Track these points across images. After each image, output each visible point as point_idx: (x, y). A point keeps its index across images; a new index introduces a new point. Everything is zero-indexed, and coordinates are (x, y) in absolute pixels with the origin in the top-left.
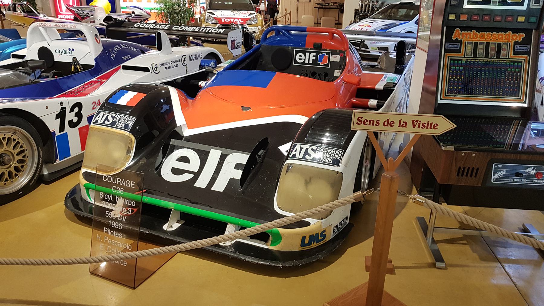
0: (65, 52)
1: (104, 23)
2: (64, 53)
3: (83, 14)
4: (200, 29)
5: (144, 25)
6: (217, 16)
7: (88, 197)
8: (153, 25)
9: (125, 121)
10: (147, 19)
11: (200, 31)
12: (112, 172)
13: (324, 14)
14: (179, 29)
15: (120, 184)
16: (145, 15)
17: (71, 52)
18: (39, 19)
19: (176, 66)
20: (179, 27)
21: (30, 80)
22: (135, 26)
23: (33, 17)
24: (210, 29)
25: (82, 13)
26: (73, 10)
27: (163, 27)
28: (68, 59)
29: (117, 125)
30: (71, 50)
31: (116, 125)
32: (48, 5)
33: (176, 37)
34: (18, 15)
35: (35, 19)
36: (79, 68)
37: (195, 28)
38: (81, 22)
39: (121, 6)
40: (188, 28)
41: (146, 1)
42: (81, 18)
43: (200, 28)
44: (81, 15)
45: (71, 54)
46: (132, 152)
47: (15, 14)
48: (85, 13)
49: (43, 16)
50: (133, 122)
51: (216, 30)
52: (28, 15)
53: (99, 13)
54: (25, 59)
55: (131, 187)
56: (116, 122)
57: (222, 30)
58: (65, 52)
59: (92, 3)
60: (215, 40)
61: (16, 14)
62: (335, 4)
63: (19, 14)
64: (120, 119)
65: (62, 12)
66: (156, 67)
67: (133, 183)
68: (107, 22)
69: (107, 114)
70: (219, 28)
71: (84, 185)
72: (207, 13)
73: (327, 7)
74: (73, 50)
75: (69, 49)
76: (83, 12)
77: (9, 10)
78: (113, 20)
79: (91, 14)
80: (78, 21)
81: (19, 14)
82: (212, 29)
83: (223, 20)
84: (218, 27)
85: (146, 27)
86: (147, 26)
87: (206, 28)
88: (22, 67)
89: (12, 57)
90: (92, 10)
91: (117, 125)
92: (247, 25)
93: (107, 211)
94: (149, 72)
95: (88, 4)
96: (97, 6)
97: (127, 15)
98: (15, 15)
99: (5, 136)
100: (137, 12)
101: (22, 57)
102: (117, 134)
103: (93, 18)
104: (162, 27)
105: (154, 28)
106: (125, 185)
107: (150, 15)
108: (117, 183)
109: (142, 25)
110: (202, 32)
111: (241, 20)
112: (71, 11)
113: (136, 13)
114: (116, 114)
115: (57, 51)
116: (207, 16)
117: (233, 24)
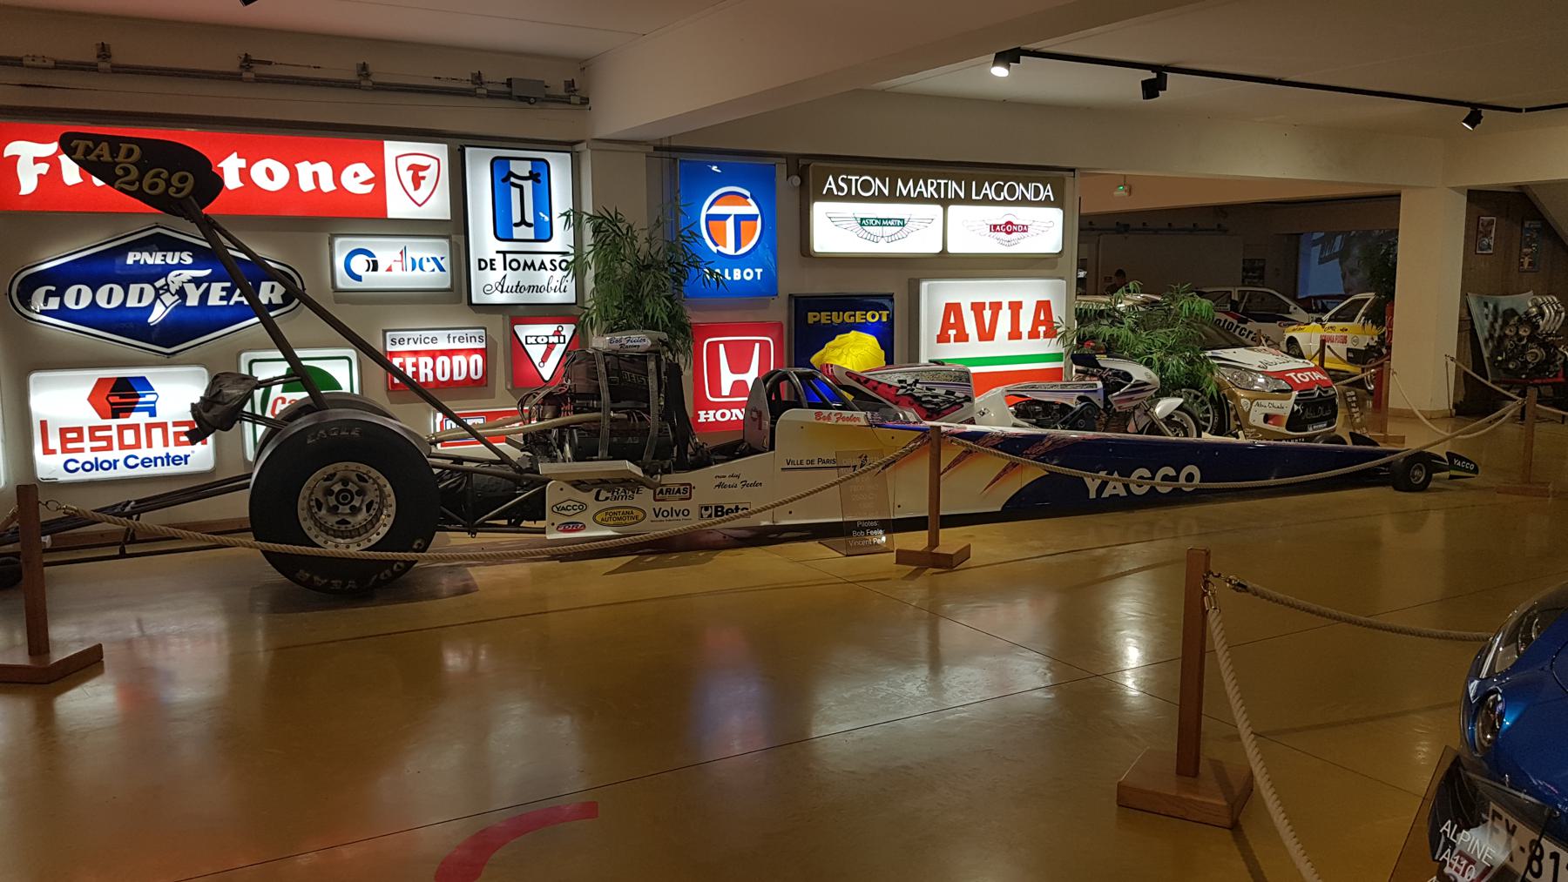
35: (920, 433)
48: (940, 391)
59: (821, 352)
61: (834, 419)
63: (844, 419)
76: (927, 389)
79: (963, 395)
81: (844, 419)
98: (826, 422)
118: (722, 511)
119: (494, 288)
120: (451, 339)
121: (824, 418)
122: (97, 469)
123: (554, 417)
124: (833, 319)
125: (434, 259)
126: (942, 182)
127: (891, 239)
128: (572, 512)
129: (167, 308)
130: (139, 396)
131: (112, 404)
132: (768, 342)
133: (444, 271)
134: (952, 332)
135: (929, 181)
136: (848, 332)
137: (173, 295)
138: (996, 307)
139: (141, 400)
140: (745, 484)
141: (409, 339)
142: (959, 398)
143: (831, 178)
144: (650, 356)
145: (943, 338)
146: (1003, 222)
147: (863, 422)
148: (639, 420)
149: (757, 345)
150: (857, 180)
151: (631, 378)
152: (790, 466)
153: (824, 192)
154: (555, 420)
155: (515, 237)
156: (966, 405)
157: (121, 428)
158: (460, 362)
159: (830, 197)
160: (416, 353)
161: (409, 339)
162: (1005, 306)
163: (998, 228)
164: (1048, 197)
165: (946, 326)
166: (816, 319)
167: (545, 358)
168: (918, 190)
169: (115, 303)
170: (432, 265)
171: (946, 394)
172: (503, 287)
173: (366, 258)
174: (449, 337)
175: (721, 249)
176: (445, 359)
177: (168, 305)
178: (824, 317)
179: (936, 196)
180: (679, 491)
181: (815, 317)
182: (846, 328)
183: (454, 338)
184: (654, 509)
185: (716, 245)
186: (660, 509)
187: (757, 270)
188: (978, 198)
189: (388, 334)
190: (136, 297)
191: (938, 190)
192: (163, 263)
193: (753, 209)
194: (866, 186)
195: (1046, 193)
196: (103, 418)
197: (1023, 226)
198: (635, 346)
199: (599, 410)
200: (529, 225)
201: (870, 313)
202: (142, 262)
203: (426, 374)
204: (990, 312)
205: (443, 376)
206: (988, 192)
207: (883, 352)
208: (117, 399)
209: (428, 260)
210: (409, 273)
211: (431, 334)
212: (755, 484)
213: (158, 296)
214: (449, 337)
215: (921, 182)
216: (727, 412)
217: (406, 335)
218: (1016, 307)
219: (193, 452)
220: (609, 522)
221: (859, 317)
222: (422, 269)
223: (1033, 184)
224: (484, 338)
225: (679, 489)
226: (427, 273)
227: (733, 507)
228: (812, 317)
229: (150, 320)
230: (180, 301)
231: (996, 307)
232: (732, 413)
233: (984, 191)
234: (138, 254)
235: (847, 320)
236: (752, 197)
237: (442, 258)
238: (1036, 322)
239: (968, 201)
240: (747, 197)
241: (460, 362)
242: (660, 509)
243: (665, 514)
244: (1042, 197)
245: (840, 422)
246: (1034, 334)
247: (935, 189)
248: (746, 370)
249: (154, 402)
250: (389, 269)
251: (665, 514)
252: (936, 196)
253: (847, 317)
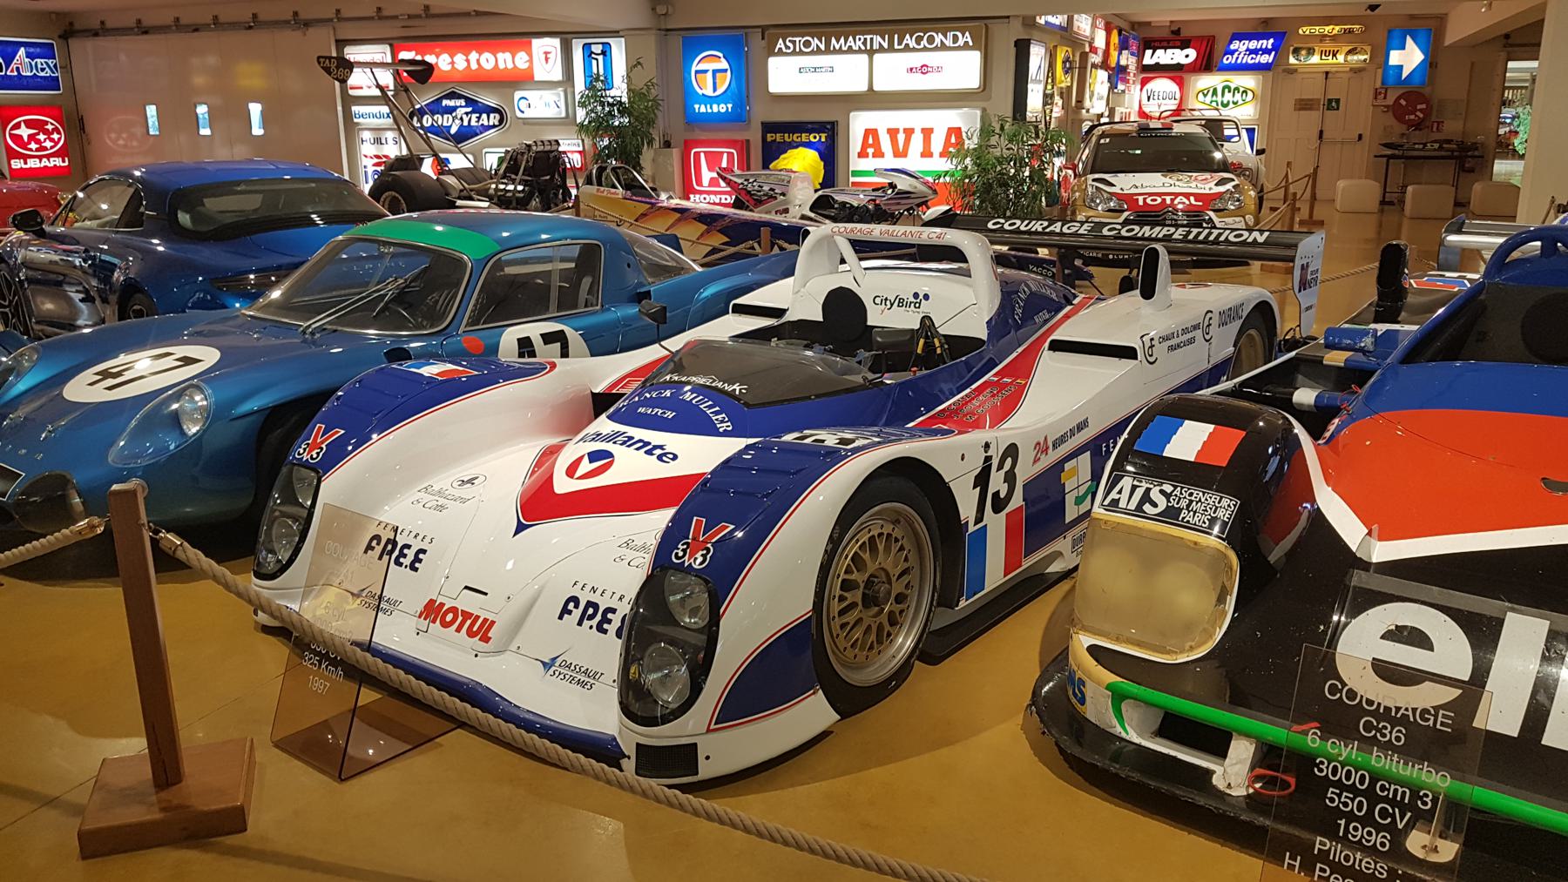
0: (901, 303)
1: (812, 215)
2: (898, 306)
3: (760, 191)
4: (1190, 232)
5: (1015, 224)
6: (1122, 189)
7: (1115, 721)
8: (1041, 224)
9: (1208, 509)
10: (927, 201)
11: (1191, 237)
12: (1182, 652)
13: (1404, 175)
14: (1006, 227)
15: (1393, 714)
16: (922, 192)
17: (920, 303)
18: (660, 205)
19: (1191, 341)
20: (1006, 221)
21: (865, 379)
22: (990, 225)
23: (643, 199)
24: (1222, 231)
25: (756, 188)
26: (736, 182)
27: (1074, 229)
28: (908, 320)
29: (1184, 518)
30: (921, 297)
31: (1180, 519)
32: (670, 169)
33: (1009, 250)
34: (609, 195)
35: (649, 206)
36: (937, 344)
37: (1173, 229)
38: (751, 210)
39: (851, 169)
40: (1151, 229)
41: (919, 155)
42: (753, 202)
43: (1187, 229)
44: (754, 194)
45: (919, 307)
46: (1231, 599)
47: (603, 192)
48: (766, 188)
49: (667, 198)
50: (1233, 512)
51: (1241, 235)
52: (633, 194)
53: (801, 190)
54: (788, 317)
55: (1438, 726)
56: (1180, 510)
57: (1261, 235)
58: (901, 303)
59: (776, 161)
60: (1111, 257)
61: (605, 193)
62: (1445, 146)
64: (1191, 501)
65: (702, 186)
66: (1152, 346)
67: (1444, 716)
68: (819, 212)
69: (1145, 485)
70: (1126, 222)
71: (1109, 685)
72: (1090, 182)
73: (1422, 153)
74: (926, 297)
75: (916, 295)
76: (759, 186)
77: (589, 181)
78: (836, 206)
80: (746, 210)
82: (1228, 232)
83: (1141, 199)
84: (1126, 219)
85: (1022, 228)
86: (1026, 226)
87: (1207, 231)
88: (776, 339)
89: (733, 312)
90: (783, 181)
91: (1184, 518)
92: (1211, 214)
93: (1331, 789)
94: (1136, 358)
95: (766, 166)
96: (794, 170)
97: (874, 194)
99: (883, 531)
100: (903, 184)
101: (778, 313)
102: (1189, 543)
103: (785, 202)
104: (1068, 228)
105: (1048, 230)
106: (1412, 719)
107: (935, 192)
108: (1381, 711)
109: (1010, 225)
110: (1195, 241)
111: (1196, 200)
112: (729, 183)
113: (899, 187)
114: (1175, 487)
115: (878, 300)
116: (1090, 189)
117: (1169, 212)
126: (868, 37)
134: (870, 151)
135: (857, 37)
138: (909, 132)
143: (781, 41)
145: (863, 154)
146: (919, 66)
147: (620, 196)
150: (800, 41)
153: (776, 51)
159: (780, 53)
163: (914, 70)
164: (966, 42)
165: (865, 145)
168: (848, 44)
179: (863, 48)
188: (900, 47)
190: (444, 120)
191: (865, 43)
193: (724, 64)
194: (807, 44)
195: (965, 39)
201: (812, 136)
206: (909, 42)
215: (851, 38)
218: (927, 133)
223: (952, 33)
228: (769, 137)
231: (909, 132)
233: (905, 42)
235: (795, 139)
236: (724, 57)
239: (891, 49)
240: (720, 58)
244: (961, 42)
247: (863, 43)
252: (863, 48)
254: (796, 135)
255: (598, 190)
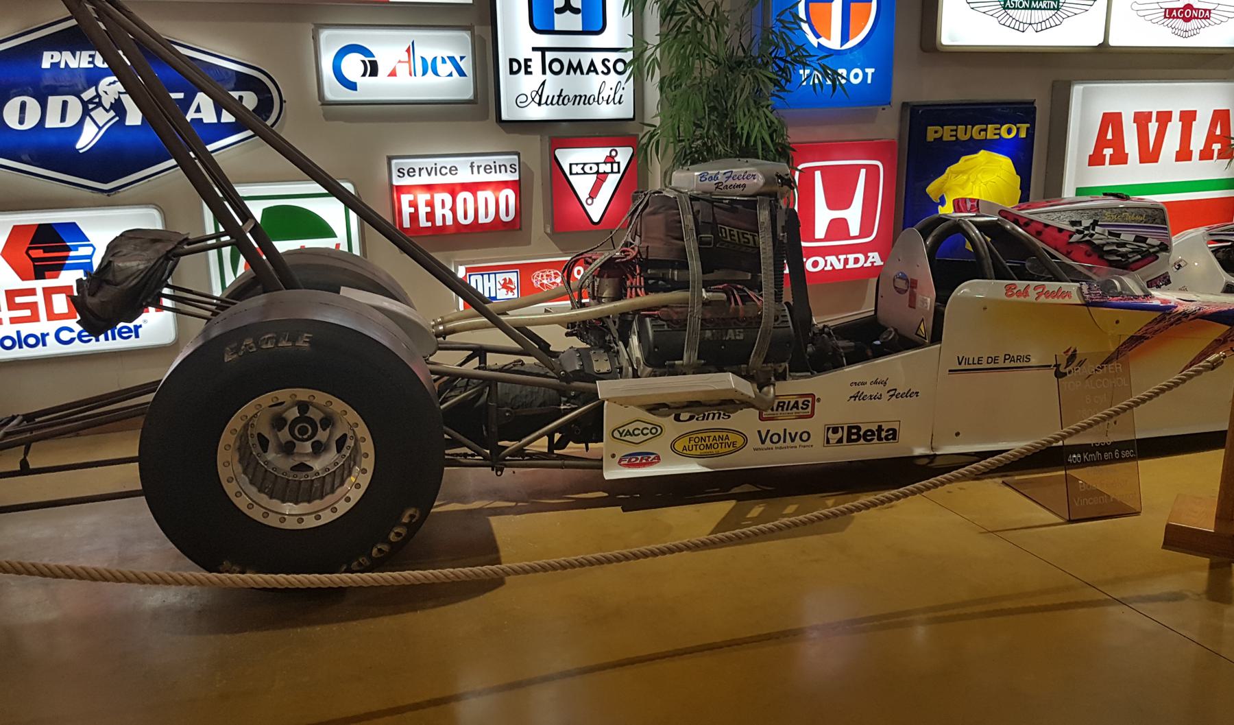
61: (1033, 295)
63: (1048, 294)
76: (1110, 233)
79: (1158, 243)
81: (1048, 294)
98: (1022, 299)
118: (857, 434)
119: (530, 99)
120: (475, 169)
121: (1019, 294)
122: (21, 347)
123: (613, 299)
124: (958, 135)
125: (452, 59)
127: (1041, 27)
128: (642, 437)
129: (100, 128)
130: (69, 249)
131: (34, 260)
132: (877, 166)
133: (465, 75)
134: (1108, 152)
136: (976, 152)
137: (107, 111)
138: (1164, 118)
139: (72, 254)
140: (894, 394)
141: (420, 170)
142: (1154, 246)
144: (762, 201)
145: (1096, 159)
147: (1076, 299)
148: (743, 303)
149: (863, 171)
151: (731, 235)
152: (963, 367)
154: (618, 304)
155: (556, 28)
156: (1162, 255)
157: (48, 292)
158: (486, 199)
160: (429, 188)
161: (420, 170)
162: (1176, 116)
163: (1174, 13)
165: (1101, 143)
166: (938, 136)
167: (593, 194)
169: (31, 122)
170: (450, 67)
171: (1135, 241)
172: (541, 96)
173: (363, 58)
174: (472, 166)
175: (823, 41)
176: (468, 195)
177: (101, 125)
178: (947, 133)
180: (796, 405)
181: (936, 132)
182: (973, 147)
183: (479, 167)
184: (759, 432)
185: (818, 36)
186: (768, 431)
187: (867, 70)
189: (394, 162)
192: (91, 66)
196: (23, 279)
197: (1205, 10)
198: (739, 186)
199: (684, 286)
200: (576, 11)
201: (1005, 127)
202: (62, 65)
203: (444, 216)
204: (1157, 124)
205: (466, 217)
207: (1018, 178)
208: (38, 253)
209: (444, 61)
210: (419, 80)
211: (449, 161)
212: (909, 394)
213: (86, 112)
214: (472, 166)
216: (820, 259)
217: (416, 163)
218: (1188, 118)
219: (145, 321)
220: (693, 452)
221: (991, 132)
222: (436, 73)
224: (517, 168)
225: (797, 402)
226: (443, 80)
227: (875, 428)
228: (932, 133)
229: (78, 146)
230: (117, 118)
231: (1164, 118)
232: (826, 261)
234: (56, 54)
235: (976, 136)
237: (462, 58)
238: (1211, 138)
241: (486, 199)
242: (768, 431)
243: (775, 438)
245: (1043, 299)
246: (1206, 154)
248: (846, 204)
249: (90, 257)
250: (393, 74)
251: (775, 438)
253: (975, 132)
254: (977, 127)
255: (1008, 288)
